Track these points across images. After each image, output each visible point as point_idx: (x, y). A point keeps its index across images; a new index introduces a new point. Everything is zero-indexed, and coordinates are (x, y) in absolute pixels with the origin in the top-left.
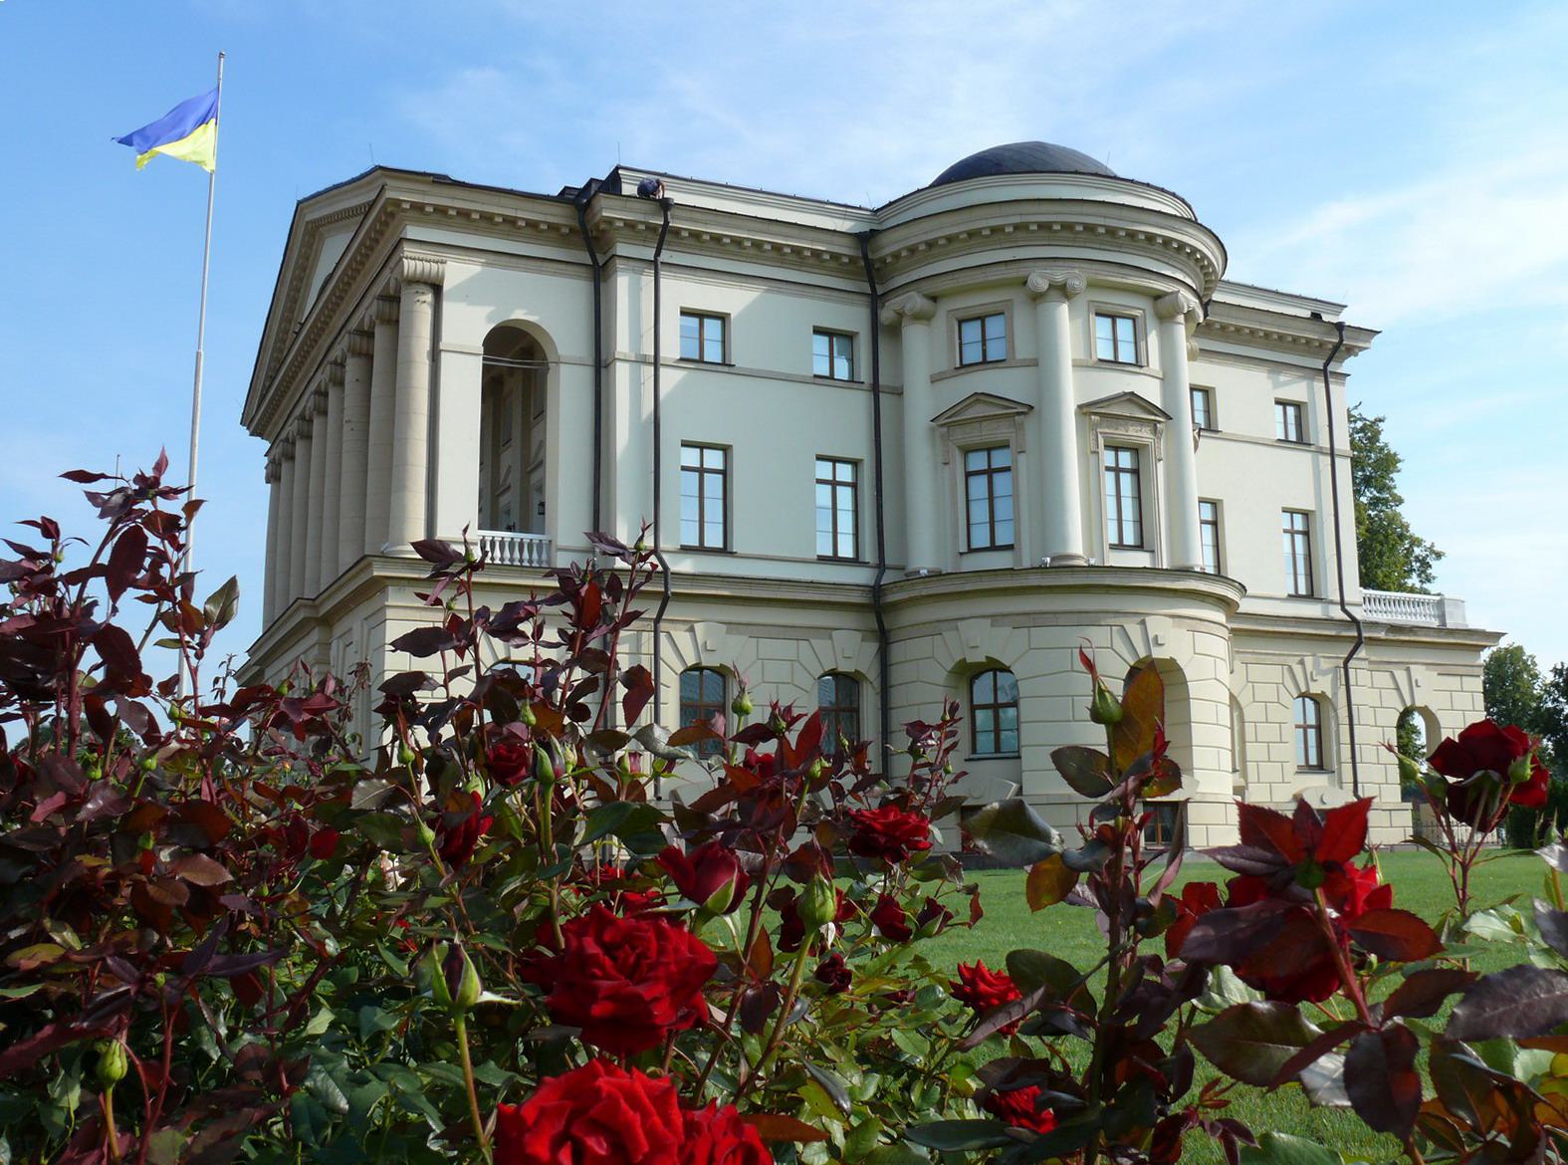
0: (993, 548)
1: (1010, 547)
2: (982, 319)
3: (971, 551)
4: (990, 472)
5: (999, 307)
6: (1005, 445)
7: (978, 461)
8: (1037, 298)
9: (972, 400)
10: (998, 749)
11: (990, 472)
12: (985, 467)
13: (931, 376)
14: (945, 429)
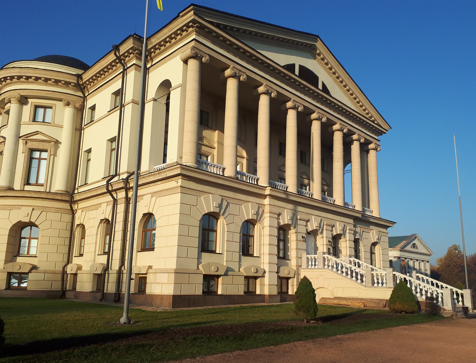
0: (37, 184)
1: (42, 185)
3: (28, 183)
6: (46, 151)
7: (37, 155)
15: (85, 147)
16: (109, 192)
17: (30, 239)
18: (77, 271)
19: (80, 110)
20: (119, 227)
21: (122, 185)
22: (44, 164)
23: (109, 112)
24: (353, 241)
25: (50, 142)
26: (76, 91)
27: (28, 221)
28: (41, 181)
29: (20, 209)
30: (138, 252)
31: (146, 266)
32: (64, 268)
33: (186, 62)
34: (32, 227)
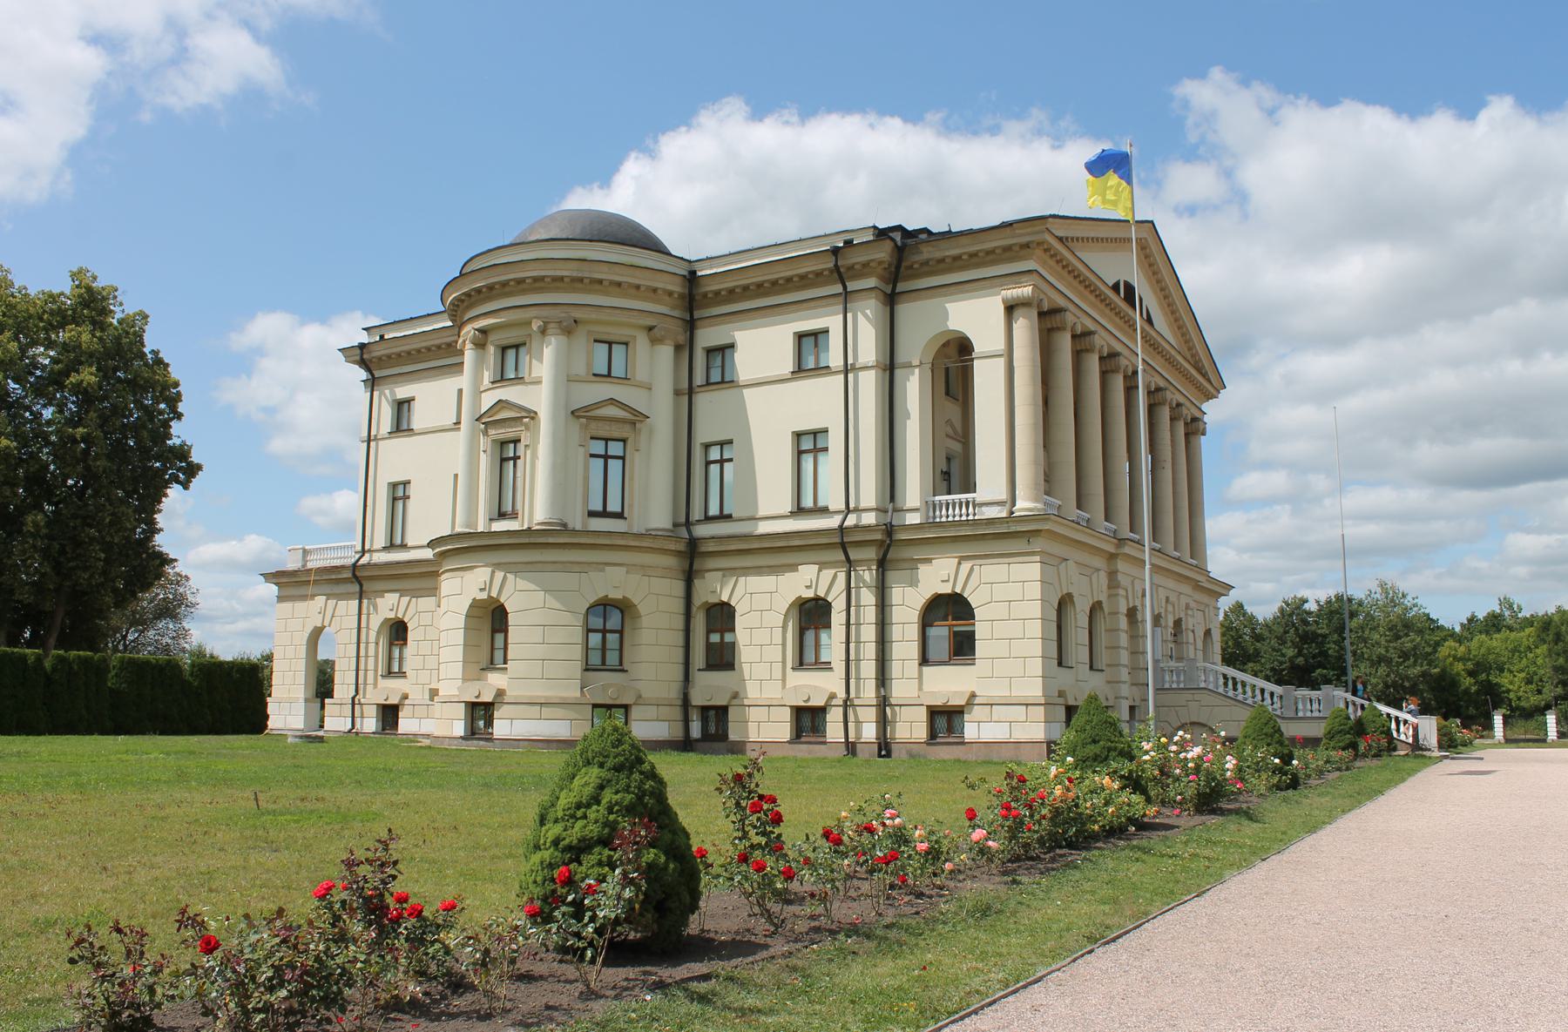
0: (604, 514)
2: (610, 344)
4: (606, 457)
5: (624, 339)
6: (624, 441)
7: (598, 447)
8: (654, 341)
9: (610, 402)
10: (604, 663)
11: (606, 457)
12: (603, 453)
13: (568, 376)
14: (584, 420)
15: (703, 435)
16: (844, 546)
19: (685, 348)
21: (878, 536)
22: (615, 466)
23: (793, 372)
26: (674, 308)
27: (621, 597)
29: (603, 570)
31: (962, 693)
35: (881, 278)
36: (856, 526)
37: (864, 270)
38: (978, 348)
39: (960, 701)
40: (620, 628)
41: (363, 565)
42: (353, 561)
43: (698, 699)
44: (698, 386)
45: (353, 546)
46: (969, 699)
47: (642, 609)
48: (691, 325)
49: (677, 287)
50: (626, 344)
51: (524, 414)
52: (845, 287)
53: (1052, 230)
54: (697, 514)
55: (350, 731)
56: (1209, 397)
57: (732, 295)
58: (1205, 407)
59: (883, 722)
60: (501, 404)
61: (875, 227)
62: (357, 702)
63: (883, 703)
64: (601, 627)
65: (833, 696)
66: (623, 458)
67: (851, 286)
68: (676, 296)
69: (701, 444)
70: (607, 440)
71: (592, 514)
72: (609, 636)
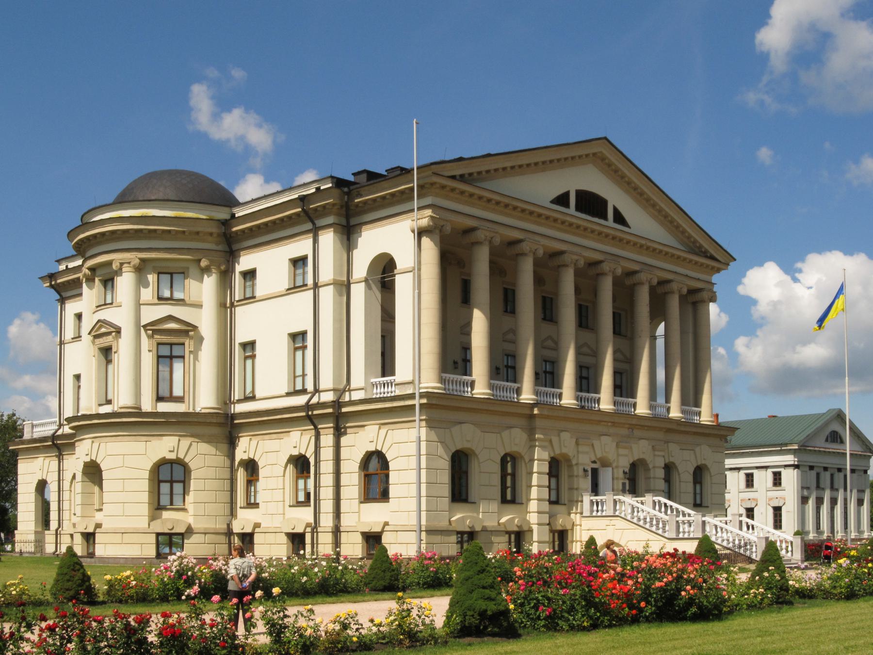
2: (171, 274)
11: (171, 357)
12: (168, 354)
14: (150, 332)
15: (241, 337)
17: (172, 482)
18: (254, 529)
20: (327, 466)
21: (330, 410)
23: (288, 289)
24: (664, 468)
25: (186, 333)
26: (217, 244)
28: (177, 392)
29: (162, 440)
30: (361, 502)
32: (228, 525)
33: (421, 233)
34: (174, 464)
35: (338, 215)
36: (318, 403)
37: (324, 211)
38: (400, 265)
39: (379, 529)
40: (183, 479)
41: (58, 436)
42: (52, 432)
43: (237, 528)
44: (238, 301)
45: (55, 422)
46: (384, 527)
47: (192, 465)
48: (232, 255)
49: (214, 229)
50: (183, 273)
51: (113, 330)
52: (314, 224)
53: (441, 173)
54: (237, 395)
55: (54, 553)
56: (718, 270)
57: (252, 232)
58: (715, 278)
59: (337, 543)
60: (101, 323)
61: (332, 177)
62: (59, 533)
63: (337, 531)
64: (169, 479)
65: (308, 525)
66: (183, 357)
67: (321, 222)
68: (215, 235)
69: (240, 344)
70: (171, 345)
71: (160, 399)
72: (175, 485)
